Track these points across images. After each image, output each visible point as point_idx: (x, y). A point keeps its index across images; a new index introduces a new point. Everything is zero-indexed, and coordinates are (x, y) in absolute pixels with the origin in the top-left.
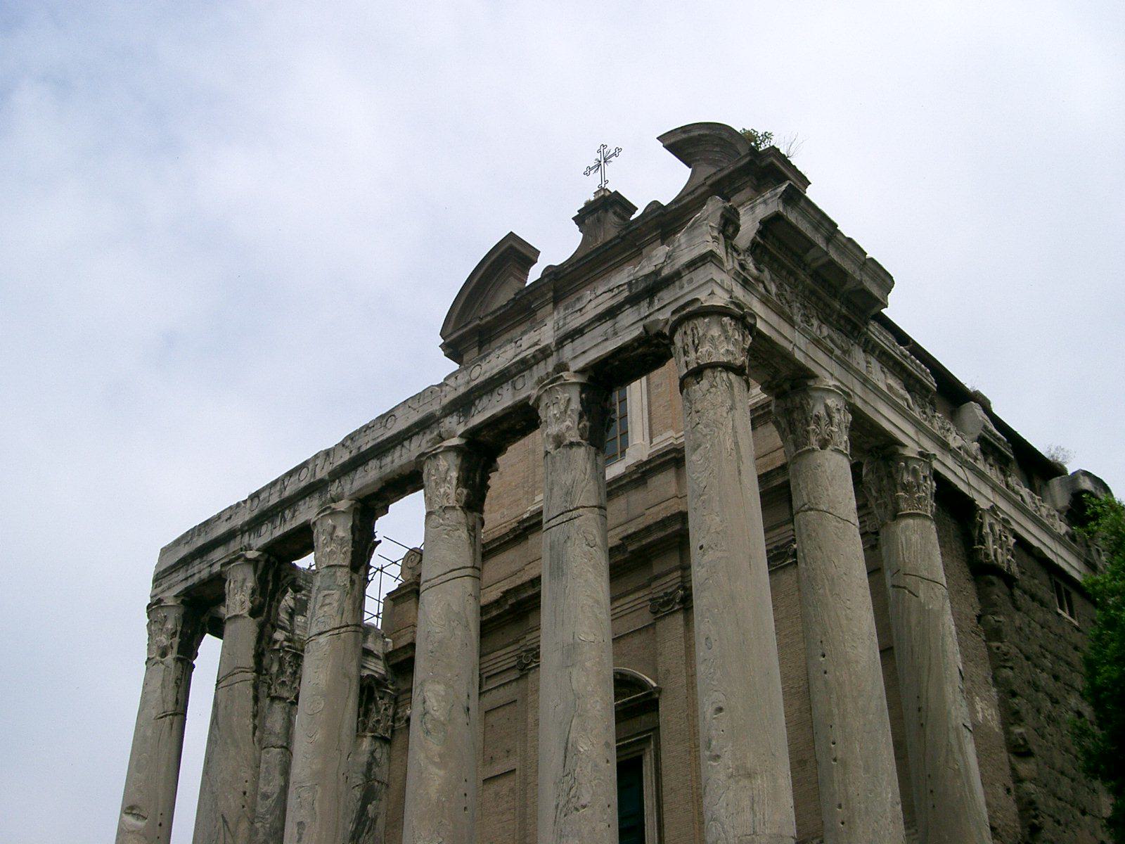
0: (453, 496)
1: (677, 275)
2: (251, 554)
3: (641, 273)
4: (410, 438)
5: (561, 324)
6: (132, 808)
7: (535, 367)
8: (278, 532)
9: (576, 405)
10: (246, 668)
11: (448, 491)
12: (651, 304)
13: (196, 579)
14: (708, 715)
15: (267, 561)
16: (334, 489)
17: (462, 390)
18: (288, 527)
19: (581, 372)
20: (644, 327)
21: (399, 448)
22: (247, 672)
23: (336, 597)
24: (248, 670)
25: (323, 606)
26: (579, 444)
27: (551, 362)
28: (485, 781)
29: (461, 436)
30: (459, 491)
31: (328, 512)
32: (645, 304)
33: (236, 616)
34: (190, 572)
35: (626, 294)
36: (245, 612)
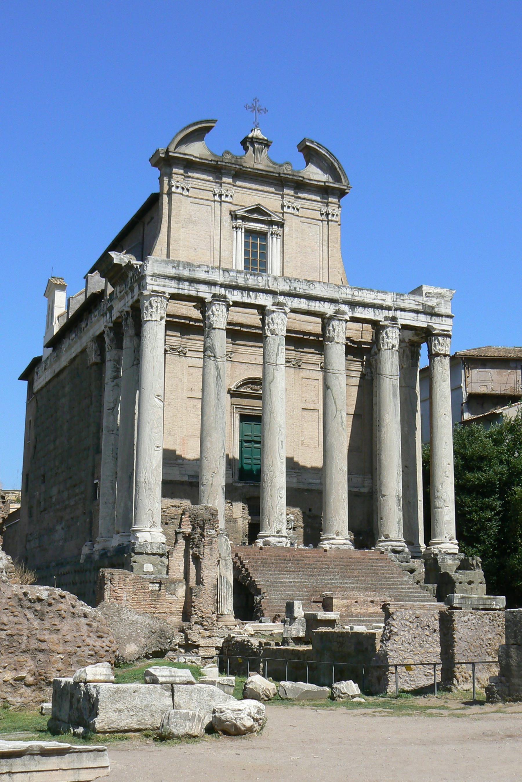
1: (442, 316)
3: (427, 303)
4: (324, 302)
5: (395, 300)
6: (158, 396)
7: (384, 311)
8: (246, 300)
12: (431, 319)
13: (186, 292)
14: (445, 464)
16: (281, 299)
17: (350, 297)
18: (253, 301)
19: (401, 325)
20: (428, 325)
21: (318, 302)
27: (391, 314)
31: (283, 311)
32: (429, 317)
34: (181, 286)
35: (420, 308)
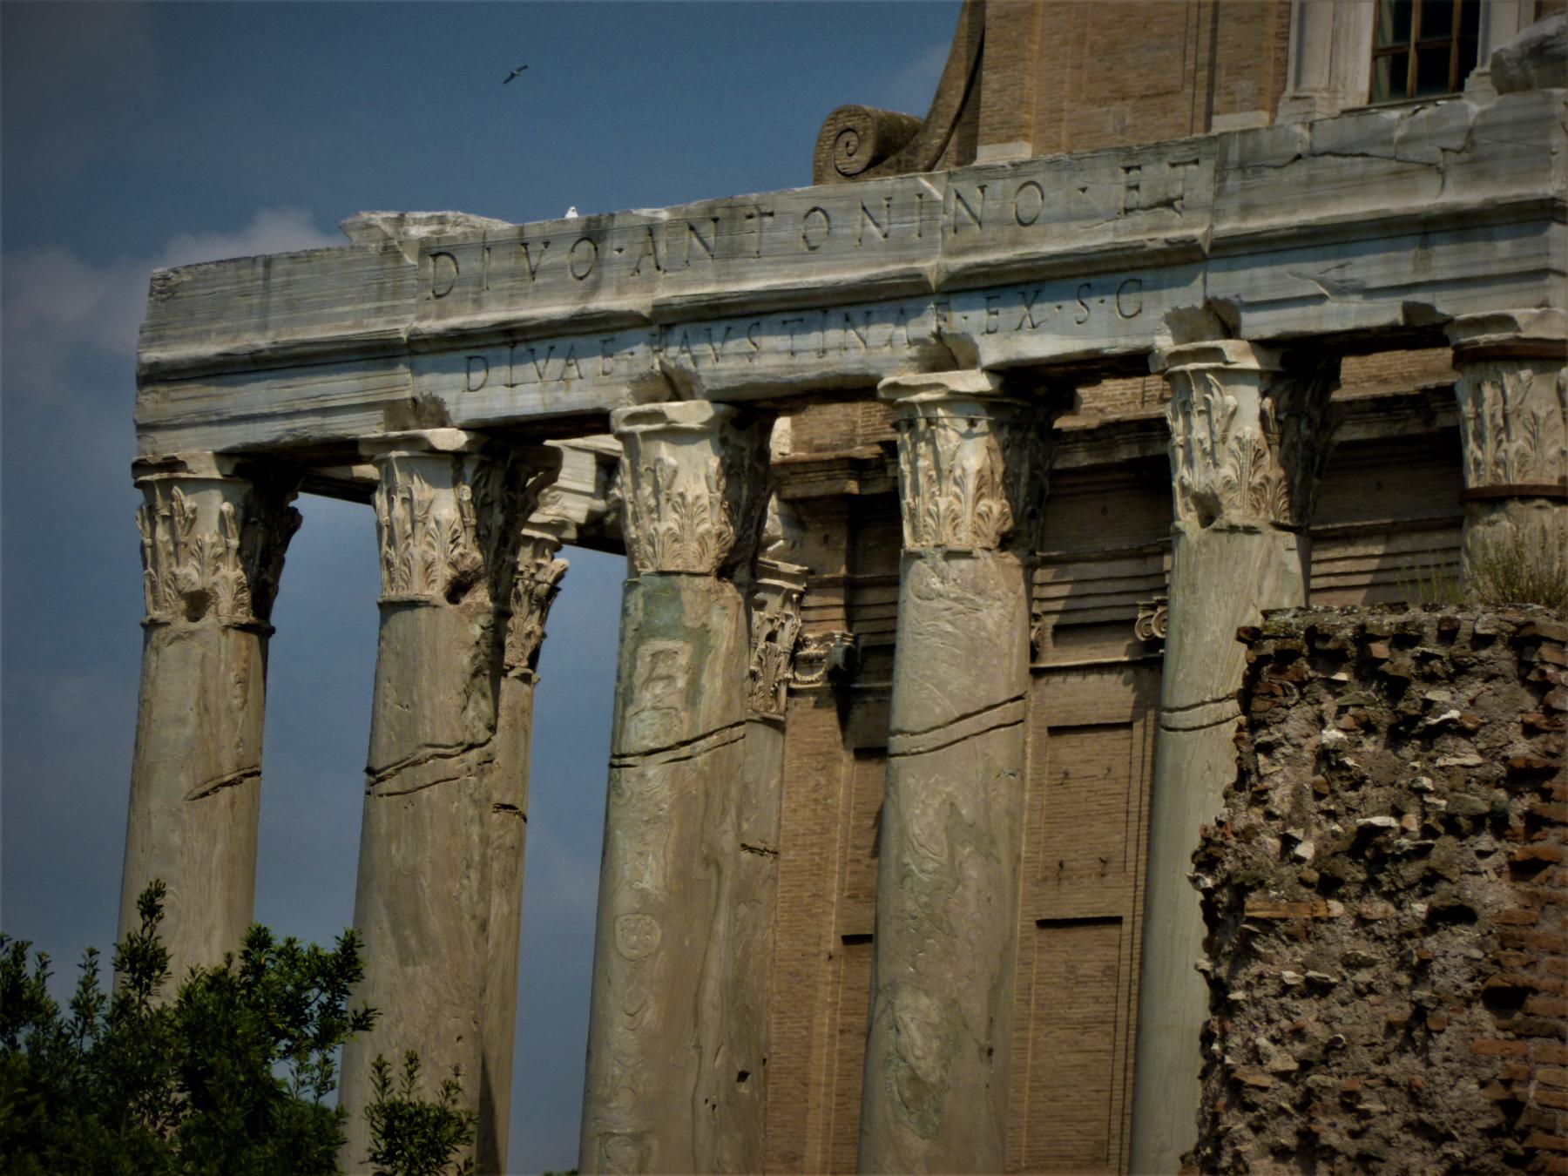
0: (967, 519)
2: (449, 438)
9: (1250, 428)
10: (447, 747)
11: (957, 506)
15: (485, 450)
22: (449, 756)
23: (683, 660)
24: (448, 751)
25: (650, 680)
26: (1250, 530)
28: (1043, 924)
29: (992, 371)
30: (983, 505)
33: (413, 604)
36: (436, 592)
